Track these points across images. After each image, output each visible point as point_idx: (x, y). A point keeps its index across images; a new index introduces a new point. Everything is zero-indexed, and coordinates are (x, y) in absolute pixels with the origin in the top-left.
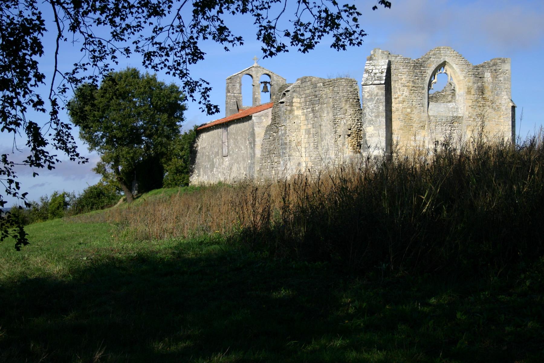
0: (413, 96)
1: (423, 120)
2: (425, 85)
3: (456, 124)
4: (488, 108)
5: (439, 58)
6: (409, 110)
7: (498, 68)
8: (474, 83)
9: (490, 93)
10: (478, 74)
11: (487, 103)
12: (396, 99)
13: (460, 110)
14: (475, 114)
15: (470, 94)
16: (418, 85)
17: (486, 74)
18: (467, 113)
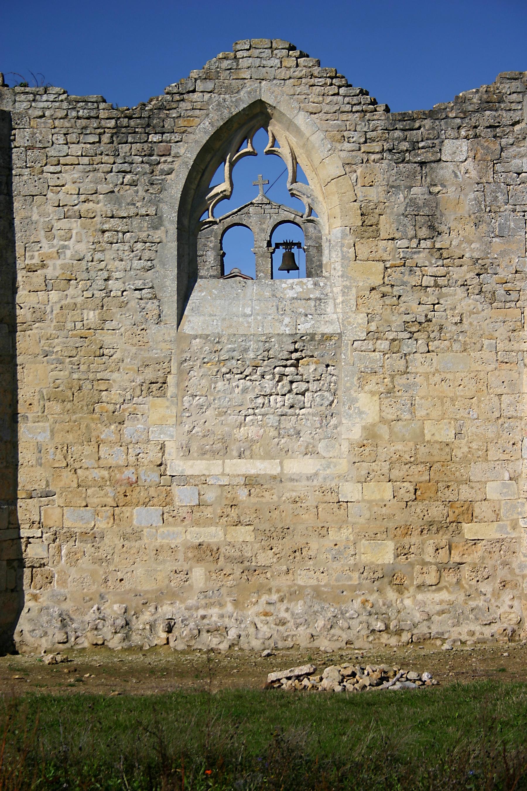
0: (109, 255)
1: (155, 354)
2: (164, 208)
3: (308, 369)
4: (460, 292)
5: (229, 90)
6: (92, 316)
7: (506, 118)
8: (392, 188)
9: (470, 228)
10: (414, 147)
11: (456, 273)
12: (31, 270)
13: (330, 309)
14: (397, 321)
15: (376, 236)
16: (132, 211)
17: (449, 146)
18: (361, 318)
